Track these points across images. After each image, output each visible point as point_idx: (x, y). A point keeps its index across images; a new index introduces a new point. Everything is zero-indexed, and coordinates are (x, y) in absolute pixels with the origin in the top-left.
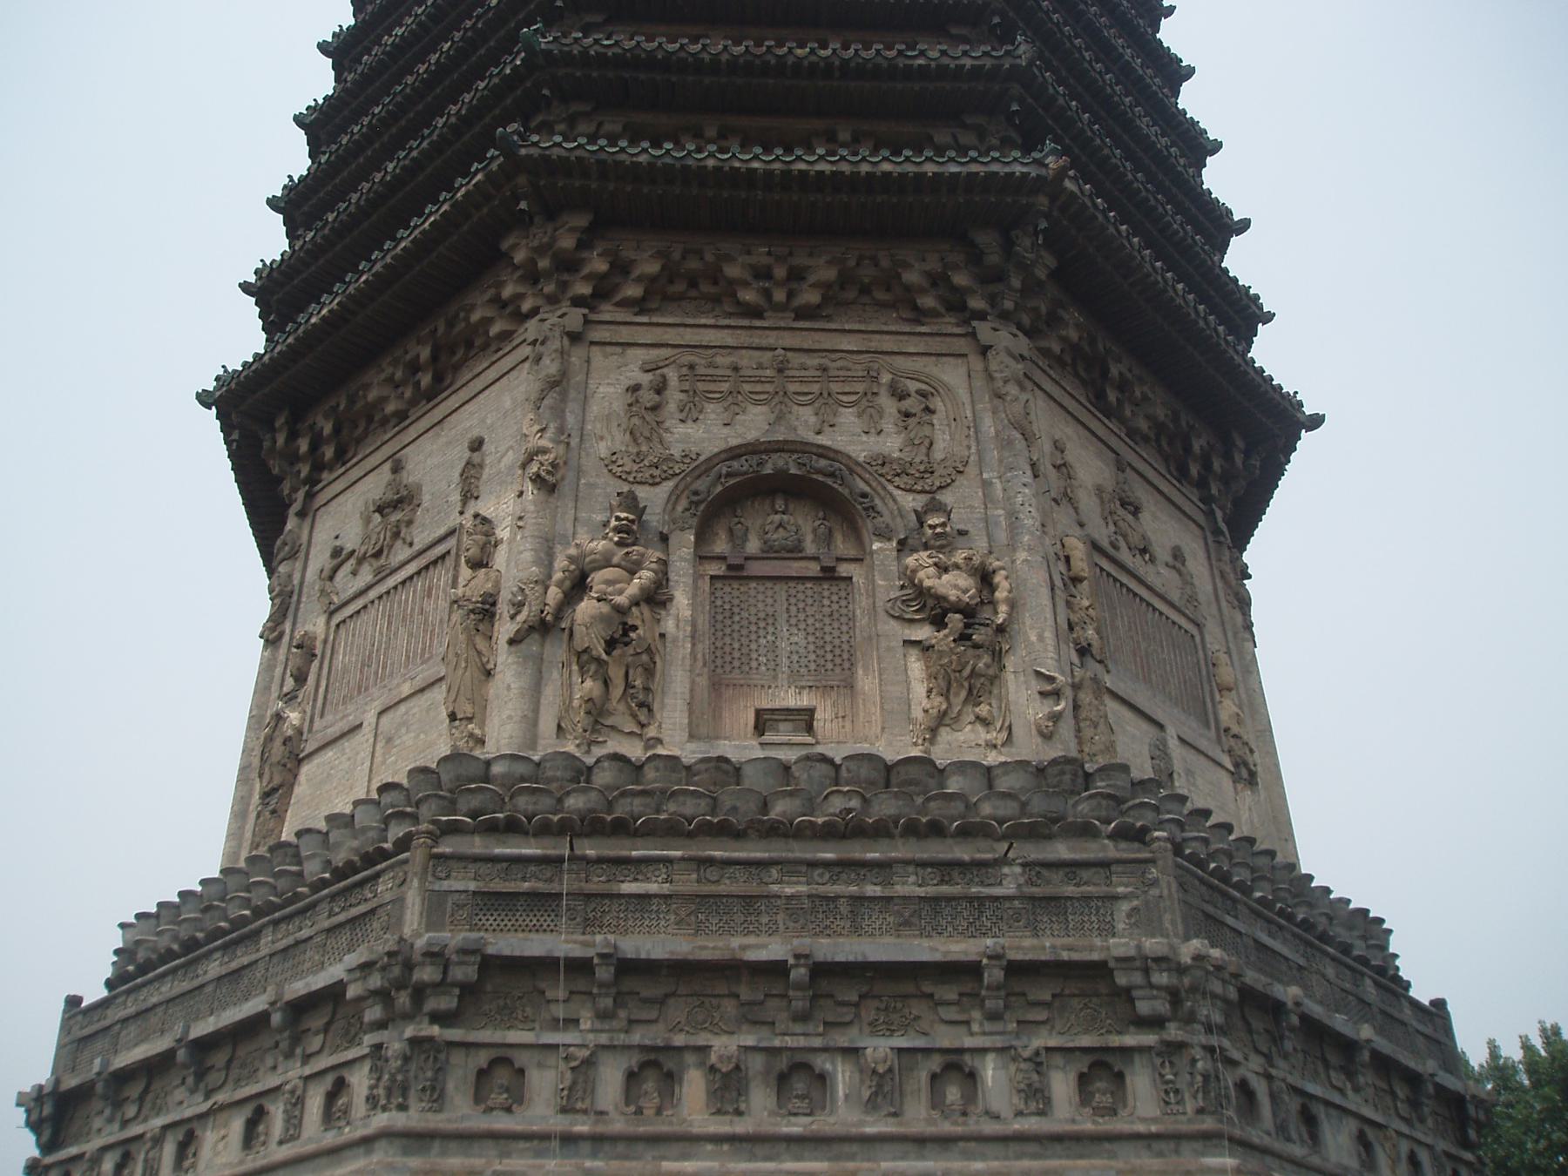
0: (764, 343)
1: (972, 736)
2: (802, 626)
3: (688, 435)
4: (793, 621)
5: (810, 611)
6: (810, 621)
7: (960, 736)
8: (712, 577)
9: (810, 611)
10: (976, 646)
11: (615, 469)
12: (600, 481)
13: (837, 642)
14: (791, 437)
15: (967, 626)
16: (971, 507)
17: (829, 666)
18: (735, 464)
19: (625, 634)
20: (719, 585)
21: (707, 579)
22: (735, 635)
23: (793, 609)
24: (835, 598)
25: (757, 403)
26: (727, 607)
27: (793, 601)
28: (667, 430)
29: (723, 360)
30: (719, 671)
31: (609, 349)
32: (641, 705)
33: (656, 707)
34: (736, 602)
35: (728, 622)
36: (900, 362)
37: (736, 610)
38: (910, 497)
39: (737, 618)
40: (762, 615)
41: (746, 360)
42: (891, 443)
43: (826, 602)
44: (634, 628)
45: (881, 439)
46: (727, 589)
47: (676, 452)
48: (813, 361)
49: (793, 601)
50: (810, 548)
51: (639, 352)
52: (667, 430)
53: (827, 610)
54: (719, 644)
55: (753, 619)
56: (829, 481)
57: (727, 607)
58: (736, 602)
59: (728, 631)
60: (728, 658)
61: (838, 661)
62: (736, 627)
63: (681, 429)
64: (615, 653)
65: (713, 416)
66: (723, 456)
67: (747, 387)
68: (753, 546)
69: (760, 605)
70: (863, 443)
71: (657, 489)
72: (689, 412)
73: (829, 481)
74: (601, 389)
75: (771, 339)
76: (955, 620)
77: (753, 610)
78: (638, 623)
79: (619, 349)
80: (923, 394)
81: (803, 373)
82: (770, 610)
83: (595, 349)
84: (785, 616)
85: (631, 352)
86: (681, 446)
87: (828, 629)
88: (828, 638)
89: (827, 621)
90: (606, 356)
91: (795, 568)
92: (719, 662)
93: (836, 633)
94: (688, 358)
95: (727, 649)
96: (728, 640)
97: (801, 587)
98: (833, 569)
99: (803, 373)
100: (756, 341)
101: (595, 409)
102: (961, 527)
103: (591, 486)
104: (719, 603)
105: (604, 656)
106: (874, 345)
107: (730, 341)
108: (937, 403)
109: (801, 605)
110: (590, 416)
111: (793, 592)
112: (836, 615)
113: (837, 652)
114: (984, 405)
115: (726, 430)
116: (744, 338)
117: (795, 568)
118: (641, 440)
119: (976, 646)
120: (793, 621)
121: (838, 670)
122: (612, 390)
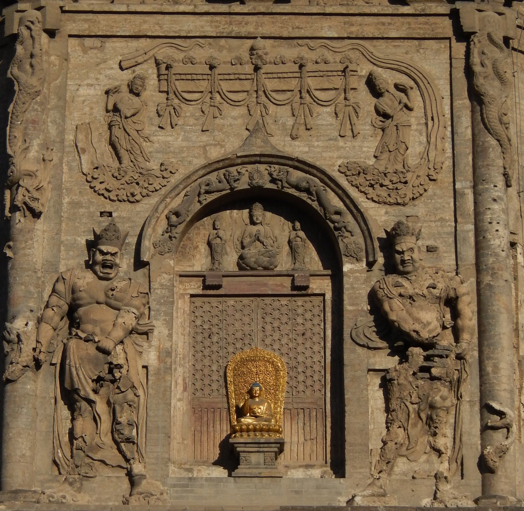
0: (243, 31)
1: (427, 467)
2: (276, 346)
3: (167, 144)
4: (268, 341)
5: (286, 329)
6: (284, 341)
7: (415, 466)
8: (192, 296)
9: (286, 329)
10: (433, 378)
11: (94, 183)
12: (84, 199)
13: (309, 362)
14: (268, 151)
15: (427, 358)
16: (442, 220)
17: (301, 387)
18: (213, 177)
19: (111, 371)
20: (198, 301)
21: (187, 297)
22: (214, 357)
23: (268, 327)
24: (308, 316)
25: (235, 103)
26: (206, 326)
27: (268, 319)
28: (147, 139)
29: (202, 53)
30: (198, 394)
31: (88, 42)
32: (129, 440)
33: (141, 441)
34: (215, 321)
35: (207, 343)
36: (380, 50)
37: (215, 330)
38: (383, 210)
39: (215, 339)
40: (239, 335)
41: (224, 54)
42: (364, 149)
43: (300, 320)
44: (119, 367)
45: (357, 143)
46: (207, 307)
47: (154, 165)
48: (290, 52)
49: (268, 319)
50: (284, 263)
51: (118, 44)
52: (147, 139)
53: (300, 328)
54: (198, 367)
55: (231, 340)
56: (304, 196)
57: (206, 326)
58: (215, 321)
59: (207, 352)
60: (207, 381)
61: (309, 382)
62: (215, 348)
63: (161, 137)
64: (102, 391)
65: (192, 121)
66: (201, 173)
67: (225, 86)
68: (230, 261)
69: (237, 324)
70: (339, 148)
71: (138, 207)
72: (168, 117)
73: (304, 196)
74: (83, 91)
75: (250, 25)
76: (417, 352)
77: (231, 330)
78: (121, 361)
79: (97, 42)
80: (400, 88)
81: (281, 68)
82: (247, 328)
83: (72, 41)
84: (261, 335)
85: (110, 44)
86: (160, 158)
87: (300, 349)
88: (300, 359)
89: (300, 340)
90: (85, 50)
91: (272, 284)
92: (198, 385)
93: (308, 353)
94: (164, 52)
95: (206, 371)
96: (207, 362)
97: (276, 304)
98: (306, 288)
99: (281, 68)
100: (236, 30)
101: (75, 118)
102: (431, 243)
103: (75, 205)
104: (198, 322)
105: (92, 396)
106: (354, 30)
107: (210, 31)
108: (416, 100)
109: (276, 324)
110: (70, 125)
111: (269, 310)
112: (308, 334)
113: (309, 372)
114: (463, 102)
115: (205, 138)
116: (223, 25)
117: (272, 284)
118: (123, 153)
119: (433, 378)
120: (268, 341)
121: (308, 392)
122: (92, 92)
